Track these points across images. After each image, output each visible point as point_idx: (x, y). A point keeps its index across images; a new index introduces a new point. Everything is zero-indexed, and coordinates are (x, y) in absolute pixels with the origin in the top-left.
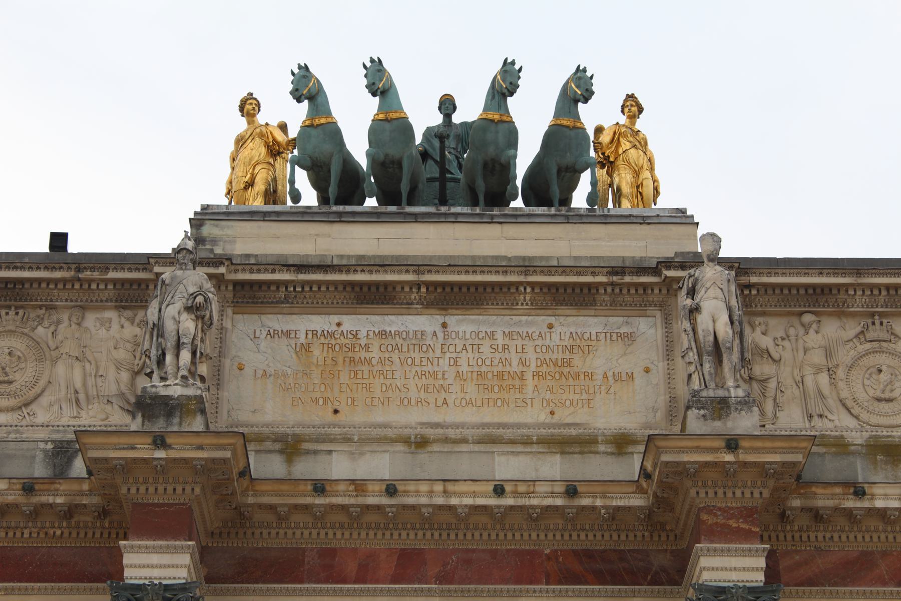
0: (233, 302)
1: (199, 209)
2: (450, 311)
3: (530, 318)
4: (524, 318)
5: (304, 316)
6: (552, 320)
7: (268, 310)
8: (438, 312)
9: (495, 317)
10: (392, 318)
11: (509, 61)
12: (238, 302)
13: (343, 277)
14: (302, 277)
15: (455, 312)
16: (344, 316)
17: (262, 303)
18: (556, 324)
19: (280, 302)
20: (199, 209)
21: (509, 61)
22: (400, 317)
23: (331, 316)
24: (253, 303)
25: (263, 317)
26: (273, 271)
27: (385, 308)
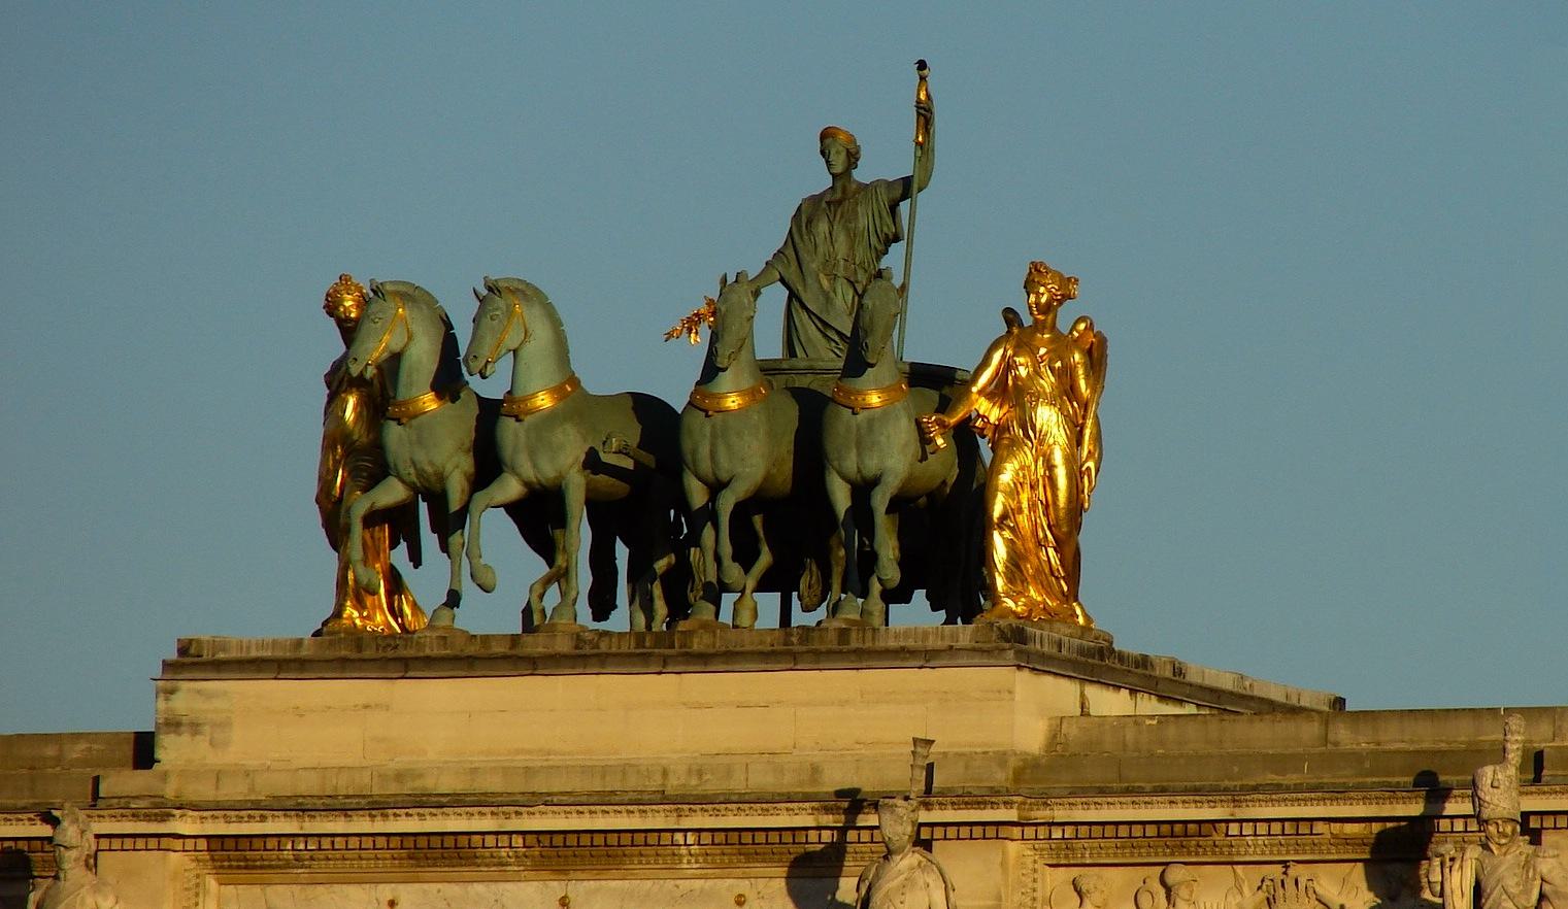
0: (215, 868)
1: (173, 655)
2: (572, 875)
3: (710, 883)
4: (698, 884)
5: (336, 887)
6: (743, 886)
7: (276, 878)
8: (552, 877)
9: (650, 883)
10: (480, 888)
11: (731, 279)
12: (222, 867)
13: (380, 826)
14: (311, 826)
15: (579, 875)
16: (401, 887)
17: (261, 867)
18: (750, 895)
19: (287, 865)
20: (173, 655)
21: (731, 279)
22: (493, 886)
23: (381, 886)
24: (246, 868)
25: (269, 889)
26: (263, 819)
27: (466, 872)
